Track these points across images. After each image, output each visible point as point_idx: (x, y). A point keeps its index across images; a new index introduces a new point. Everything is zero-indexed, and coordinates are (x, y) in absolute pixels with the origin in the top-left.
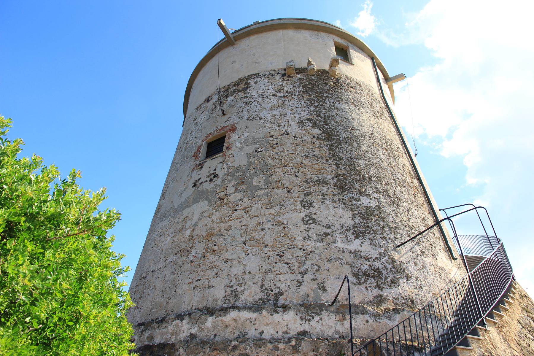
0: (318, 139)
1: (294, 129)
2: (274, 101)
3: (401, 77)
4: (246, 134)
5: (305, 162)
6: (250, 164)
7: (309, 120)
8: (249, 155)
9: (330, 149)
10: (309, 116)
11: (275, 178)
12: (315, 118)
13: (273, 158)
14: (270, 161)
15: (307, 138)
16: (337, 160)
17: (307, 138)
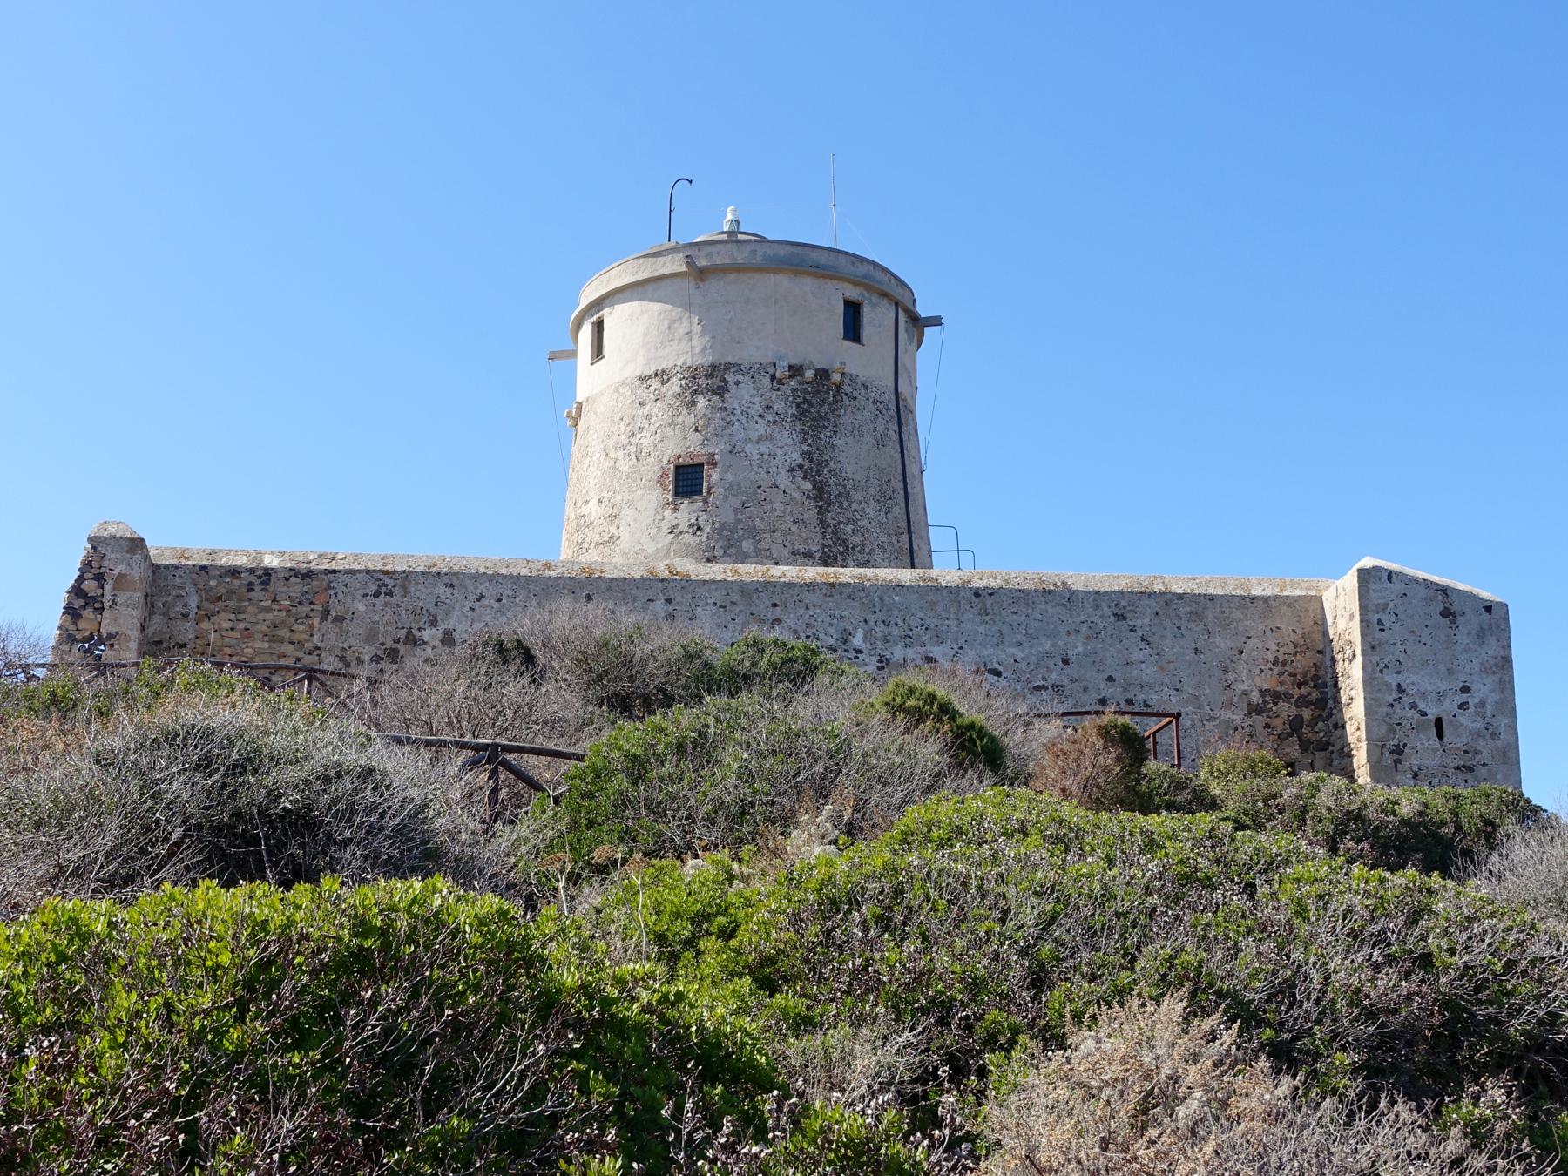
0: (808, 497)
1: (784, 480)
2: (761, 428)
3: (936, 321)
4: (730, 477)
5: (794, 528)
6: (738, 521)
7: (801, 466)
8: (735, 510)
9: (819, 513)
10: (800, 461)
11: (763, 545)
12: (807, 465)
13: (762, 519)
14: (758, 522)
15: (796, 495)
16: (823, 524)
17: (796, 495)
